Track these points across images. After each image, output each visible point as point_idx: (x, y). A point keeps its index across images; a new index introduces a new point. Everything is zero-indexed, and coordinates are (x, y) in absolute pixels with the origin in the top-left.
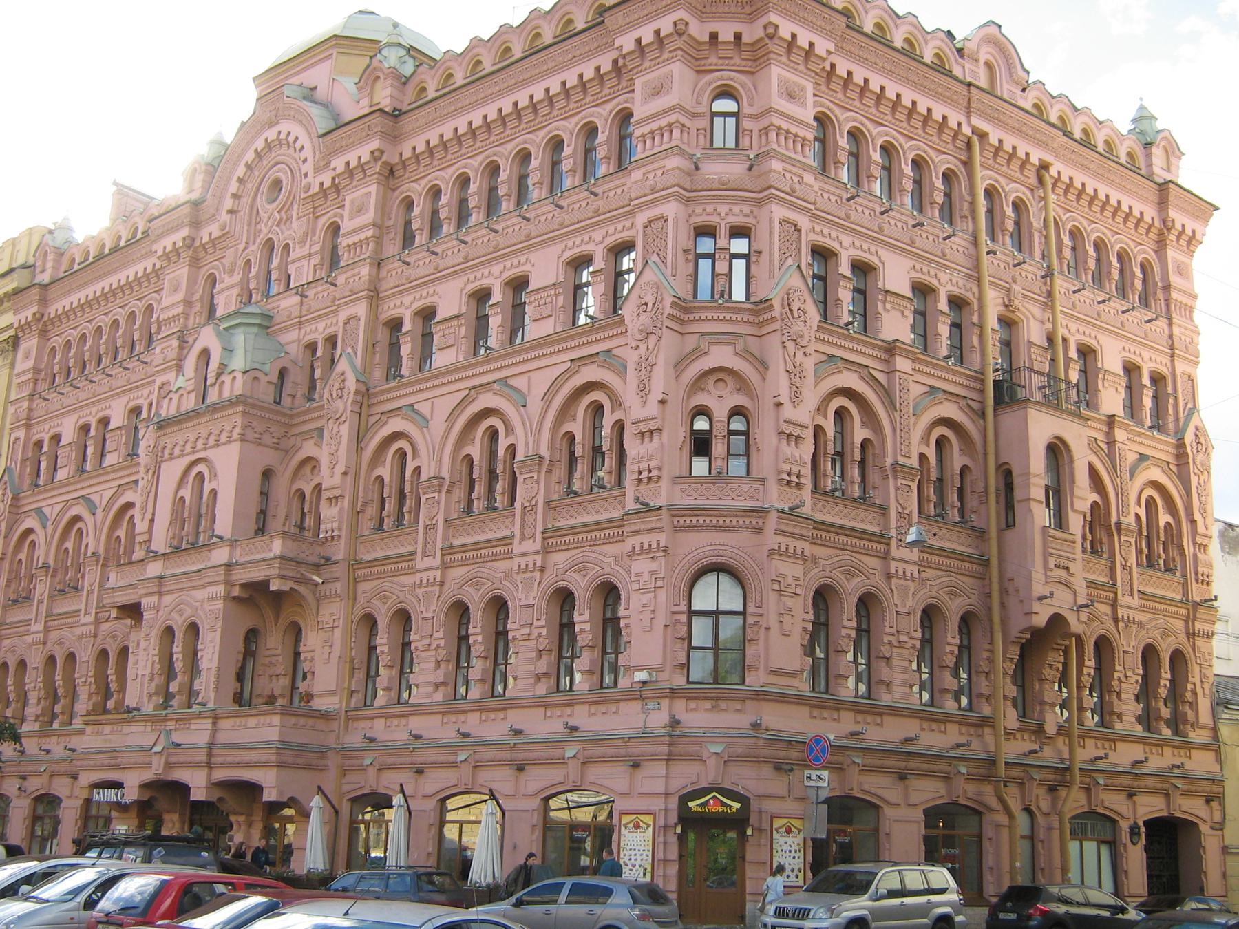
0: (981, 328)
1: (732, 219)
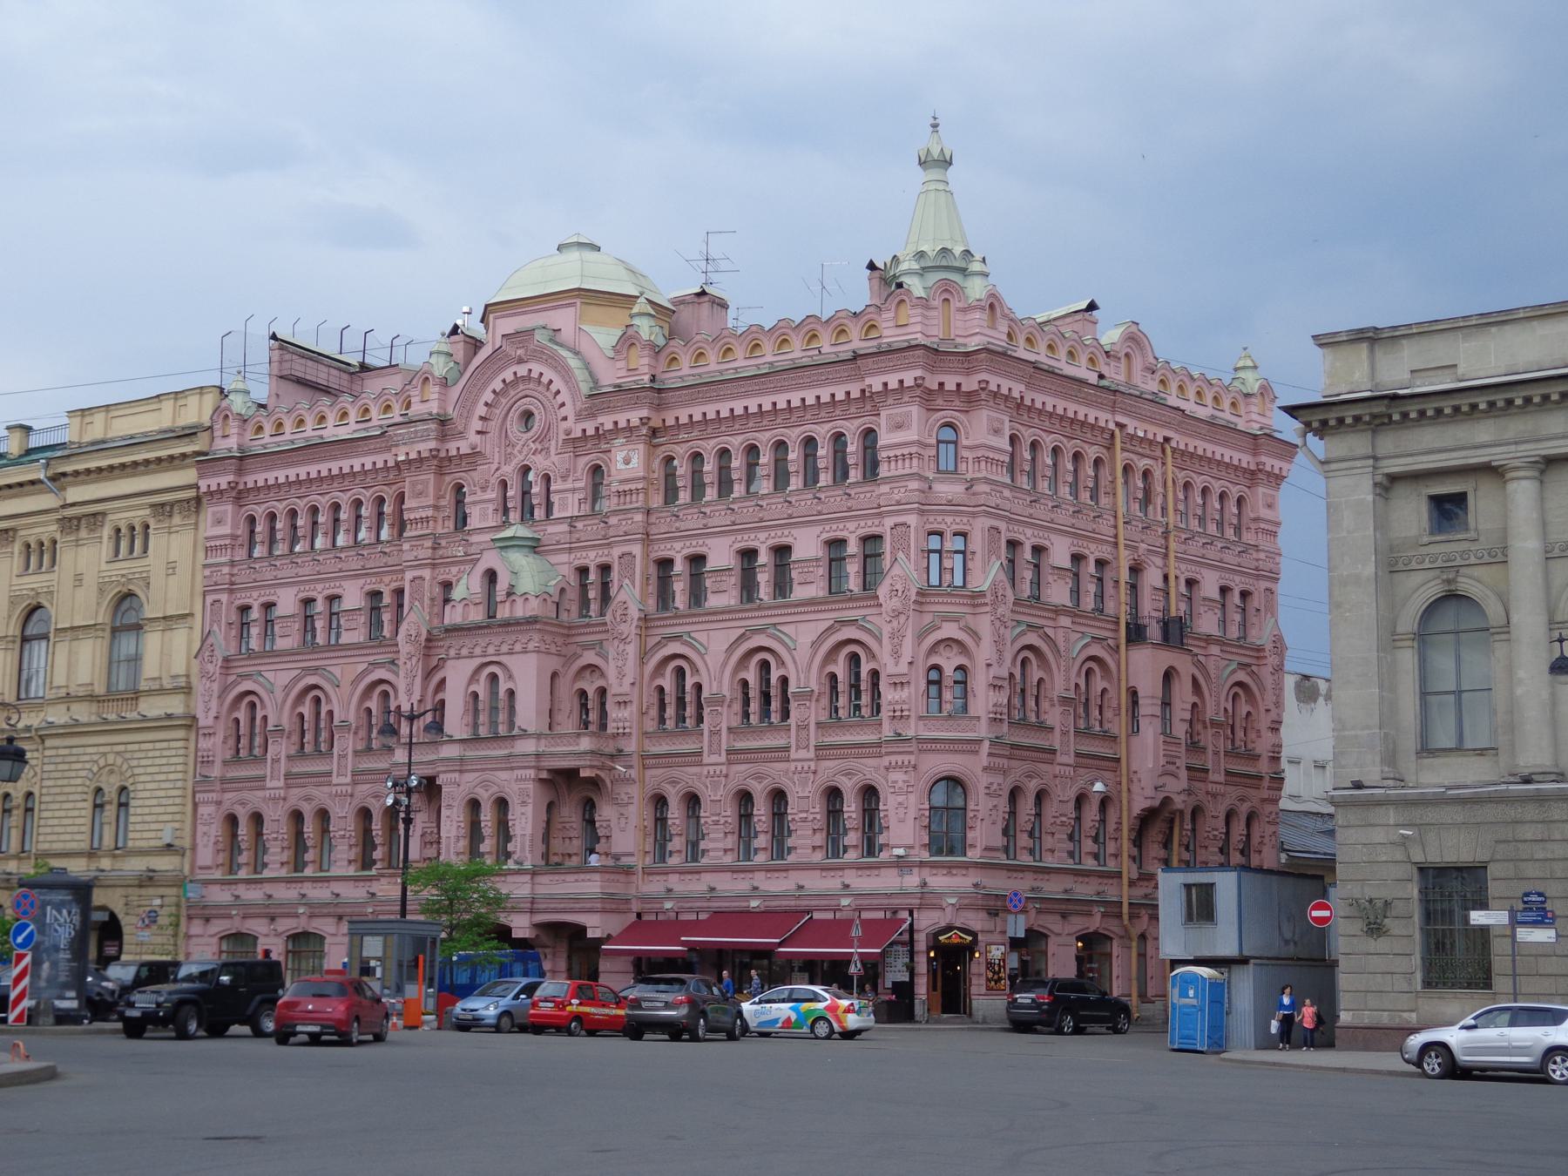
1: (956, 527)
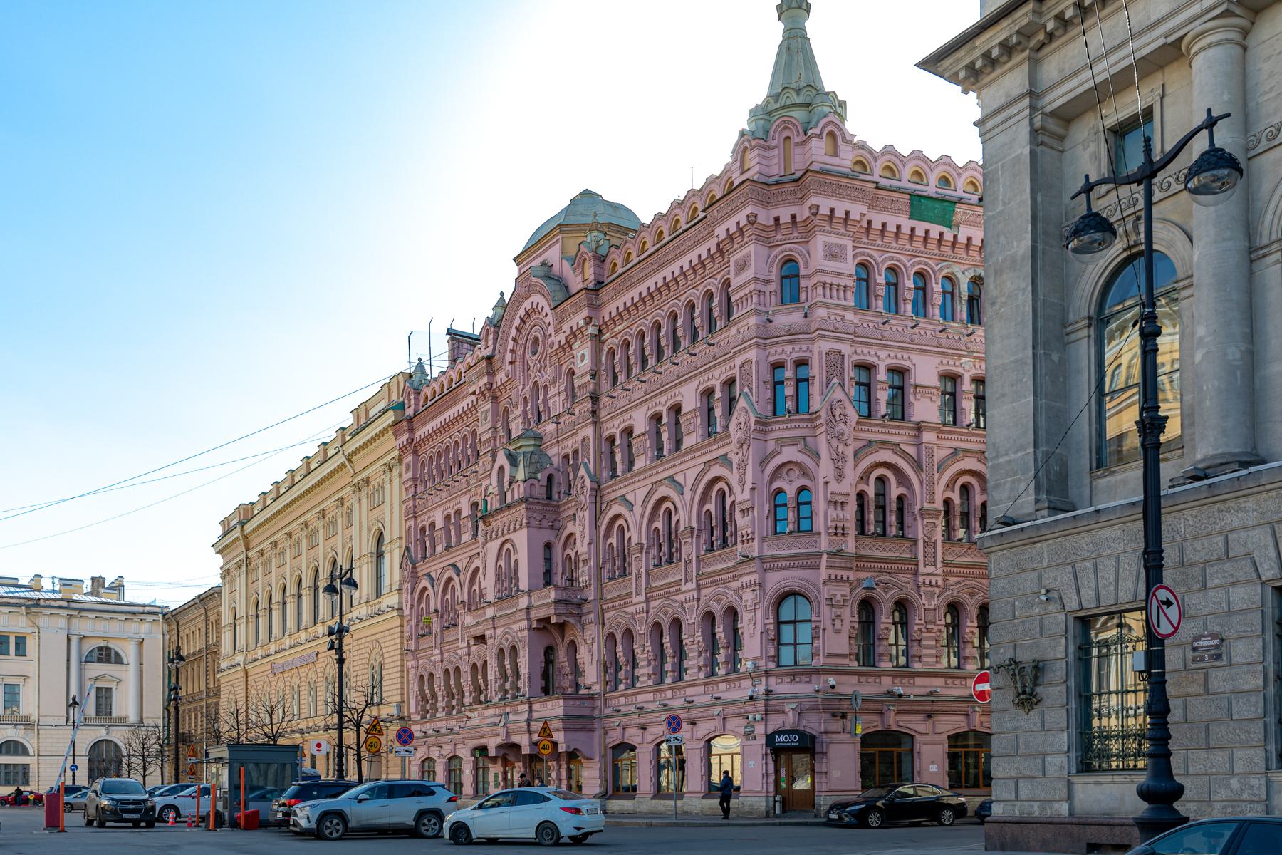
1: (795, 355)
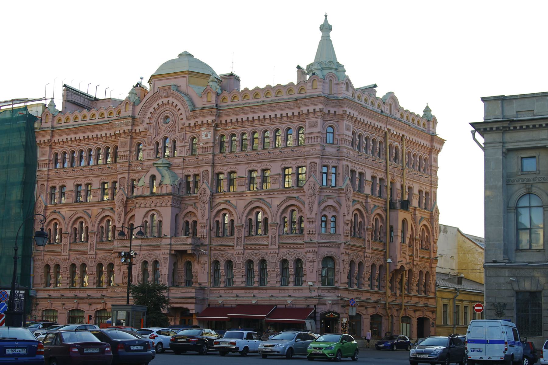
0: (387, 187)
1: (333, 164)
